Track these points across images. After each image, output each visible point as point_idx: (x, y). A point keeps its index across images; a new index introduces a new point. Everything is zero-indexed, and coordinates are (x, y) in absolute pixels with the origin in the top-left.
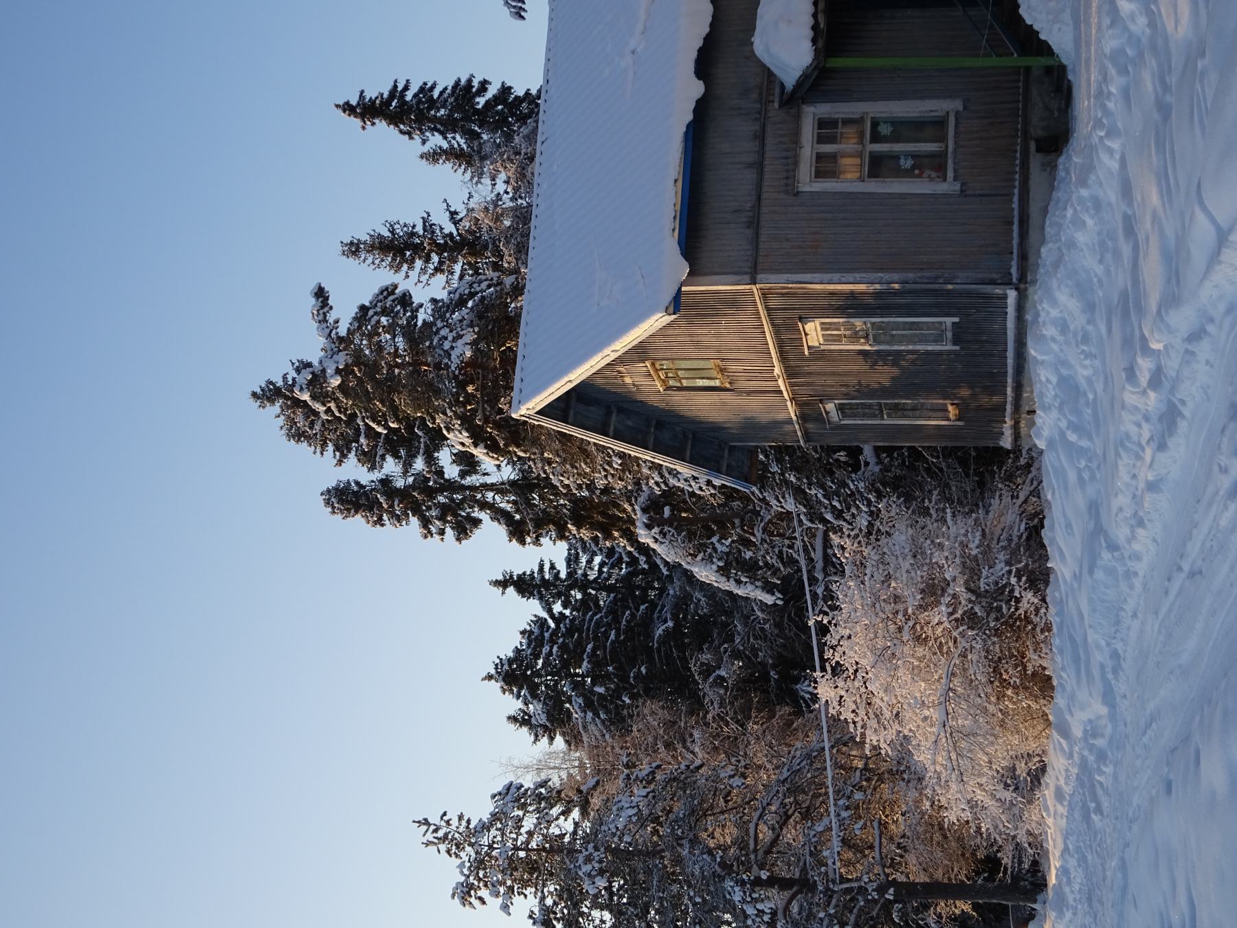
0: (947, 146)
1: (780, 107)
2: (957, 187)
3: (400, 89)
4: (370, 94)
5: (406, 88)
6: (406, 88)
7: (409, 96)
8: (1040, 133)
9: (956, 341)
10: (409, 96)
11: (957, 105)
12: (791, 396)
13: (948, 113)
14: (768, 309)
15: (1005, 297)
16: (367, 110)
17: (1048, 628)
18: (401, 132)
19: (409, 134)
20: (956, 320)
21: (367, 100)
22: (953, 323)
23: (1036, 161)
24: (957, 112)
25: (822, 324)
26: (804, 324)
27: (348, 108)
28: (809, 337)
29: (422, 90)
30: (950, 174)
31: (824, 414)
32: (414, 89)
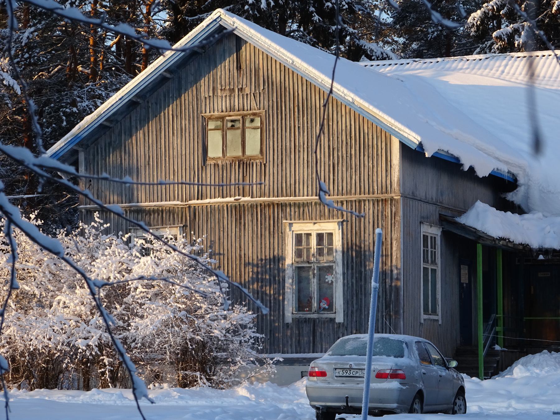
0: (431, 315)
1: (440, 214)
2: (422, 321)
9: (298, 322)
11: (440, 323)
12: (192, 206)
13: (438, 315)
14: (360, 201)
17: (185, 383)
22: (332, 320)
24: (437, 320)
25: (330, 235)
26: (338, 223)
28: (312, 224)
30: (426, 317)
31: (157, 227)
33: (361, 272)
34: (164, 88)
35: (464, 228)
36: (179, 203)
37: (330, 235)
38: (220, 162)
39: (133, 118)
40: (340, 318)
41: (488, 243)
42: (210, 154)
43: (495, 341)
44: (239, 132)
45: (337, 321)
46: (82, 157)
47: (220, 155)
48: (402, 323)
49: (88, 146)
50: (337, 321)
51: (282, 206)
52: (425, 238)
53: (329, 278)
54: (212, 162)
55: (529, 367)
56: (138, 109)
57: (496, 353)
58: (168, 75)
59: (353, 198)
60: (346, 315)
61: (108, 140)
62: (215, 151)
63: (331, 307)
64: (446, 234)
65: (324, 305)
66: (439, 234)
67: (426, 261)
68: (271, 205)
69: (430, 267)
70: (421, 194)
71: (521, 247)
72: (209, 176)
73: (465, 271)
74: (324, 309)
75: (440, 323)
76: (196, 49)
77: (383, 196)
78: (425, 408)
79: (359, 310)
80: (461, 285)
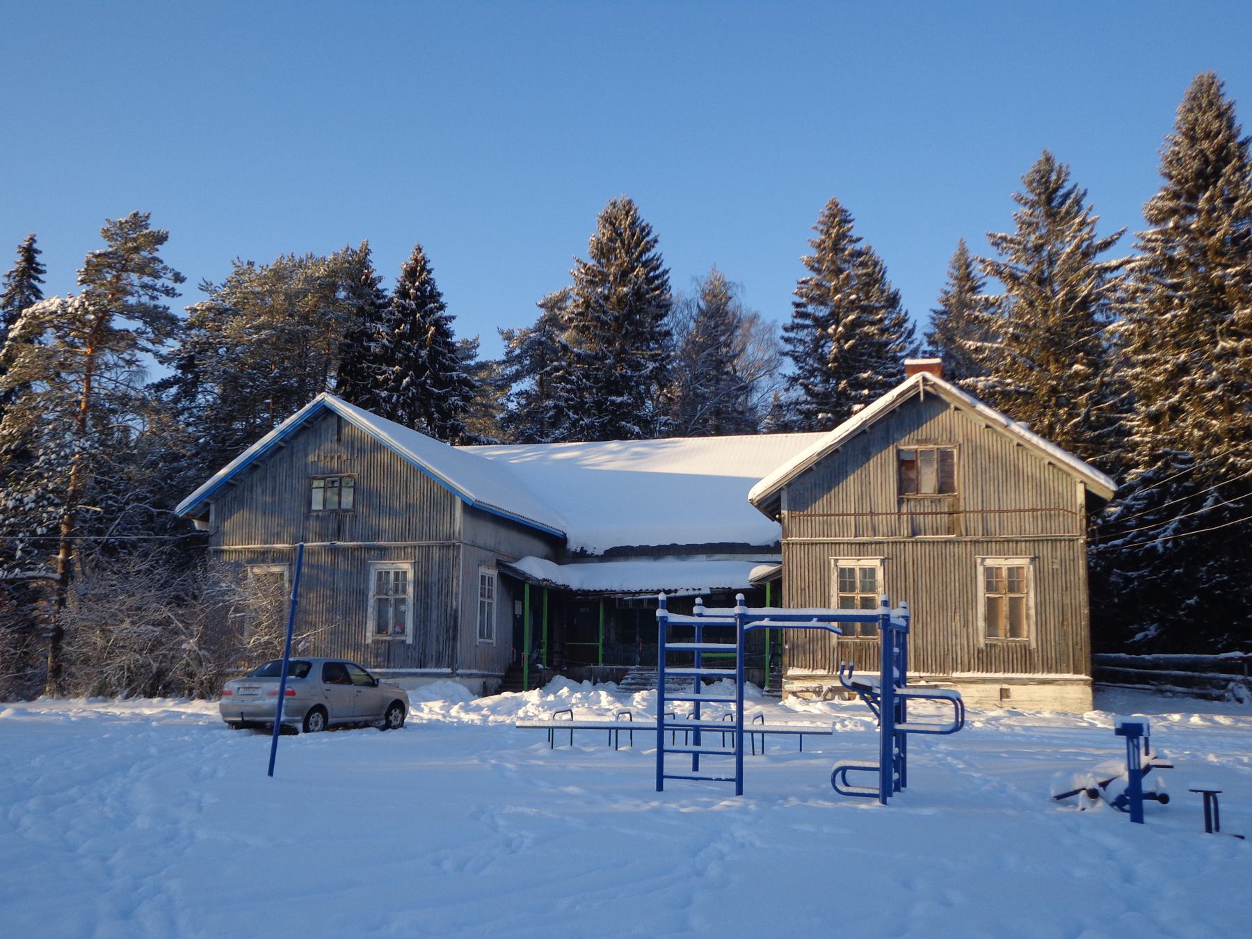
2: (478, 644)
3: (40, 276)
4: (39, 258)
5: (40, 281)
6: (40, 281)
7: (36, 283)
8: (487, 683)
9: (375, 642)
10: (36, 283)
11: (494, 645)
14: (429, 547)
15: (437, 666)
16: (29, 253)
18: (11, 272)
19: (9, 276)
20: (409, 640)
21: (35, 255)
22: (403, 642)
23: (478, 683)
25: (405, 573)
27: (32, 240)
29: (39, 291)
30: (481, 640)
32: (39, 286)
33: (428, 604)
34: (278, 456)
35: (515, 570)
36: (287, 545)
37: (405, 573)
38: (320, 514)
39: (255, 478)
40: (409, 640)
41: (534, 583)
42: (314, 507)
43: (539, 660)
44: (336, 489)
45: (407, 642)
46: (212, 508)
47: (321, 508)
48: (458, 645)
49: (218, 500)
50: (407, 642)
51: (369, 548)
52: (483, 578)
53: (403, 608)
54: (315, 514)
55: (226, 689)
56: (259, 471)
57: (538, 671)
58: (283, 445)
59: (424, 543)
60: (415, 637)
61: (234, 495)
62: (317, 505)
63: (403, 632)
64: (501, 575)
65: (398, 629)
66: (496, 575)
67: (482, 595)
68: (359, 548)
69: (487, 601)
70: (481, 542)
71: (562, 587)
72: (313, 525)
73: (518, 605)
74: (398, 633)
75: (494, 645)
76: (305, 423)
77: (447, 543)
78: (331, 720)
79: (425, 634)
80: (515, 616)
